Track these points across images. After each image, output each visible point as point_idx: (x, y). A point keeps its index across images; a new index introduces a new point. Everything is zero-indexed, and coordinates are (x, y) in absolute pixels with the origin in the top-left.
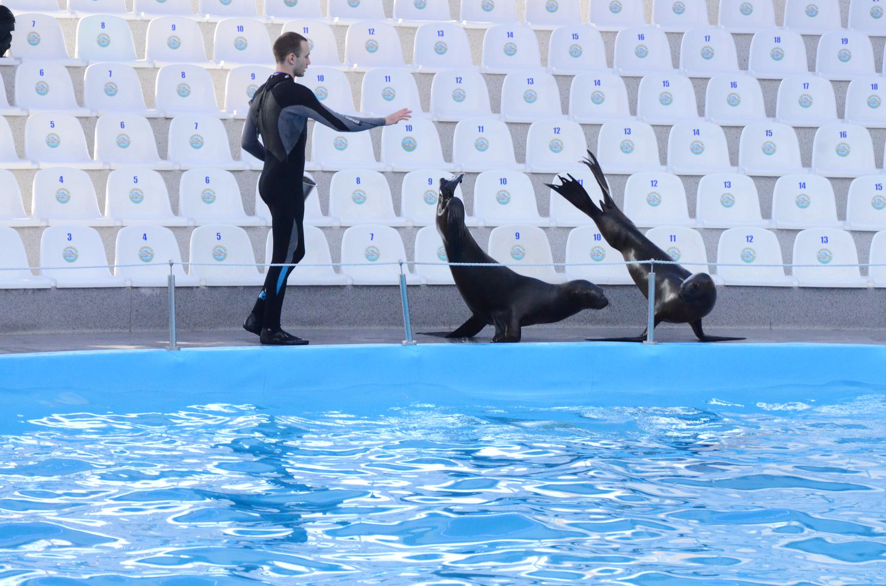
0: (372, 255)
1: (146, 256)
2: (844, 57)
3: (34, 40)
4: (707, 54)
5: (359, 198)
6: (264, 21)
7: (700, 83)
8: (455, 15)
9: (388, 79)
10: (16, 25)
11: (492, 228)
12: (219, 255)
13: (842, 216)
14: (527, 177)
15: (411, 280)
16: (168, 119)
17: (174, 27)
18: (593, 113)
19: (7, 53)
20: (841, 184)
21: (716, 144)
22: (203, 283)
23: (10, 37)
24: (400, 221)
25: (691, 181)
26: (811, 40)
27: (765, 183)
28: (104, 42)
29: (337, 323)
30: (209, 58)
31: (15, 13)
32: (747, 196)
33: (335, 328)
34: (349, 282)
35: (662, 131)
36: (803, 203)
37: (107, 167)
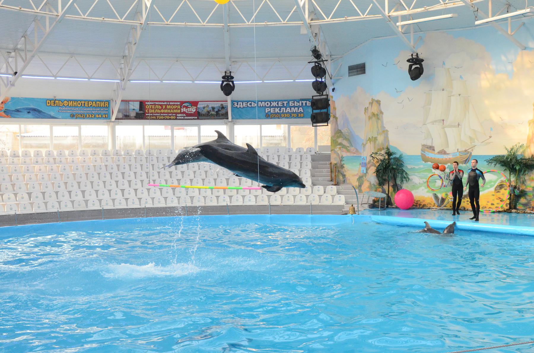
0: (53, 207)
1: (11, 209)
2: (136, 168)
4: (112, 169)
5: (50, 197)
7: (111, 174)
12: (25, 208)
13: (136, 195)
18: (105, 179)
20: (136, 190)
21: (114, 184)
25: (110, 191)
26: (130, 165)
27: (123, 191)
32: (120, 193)
35: (104, 182)
36: (129, 194)
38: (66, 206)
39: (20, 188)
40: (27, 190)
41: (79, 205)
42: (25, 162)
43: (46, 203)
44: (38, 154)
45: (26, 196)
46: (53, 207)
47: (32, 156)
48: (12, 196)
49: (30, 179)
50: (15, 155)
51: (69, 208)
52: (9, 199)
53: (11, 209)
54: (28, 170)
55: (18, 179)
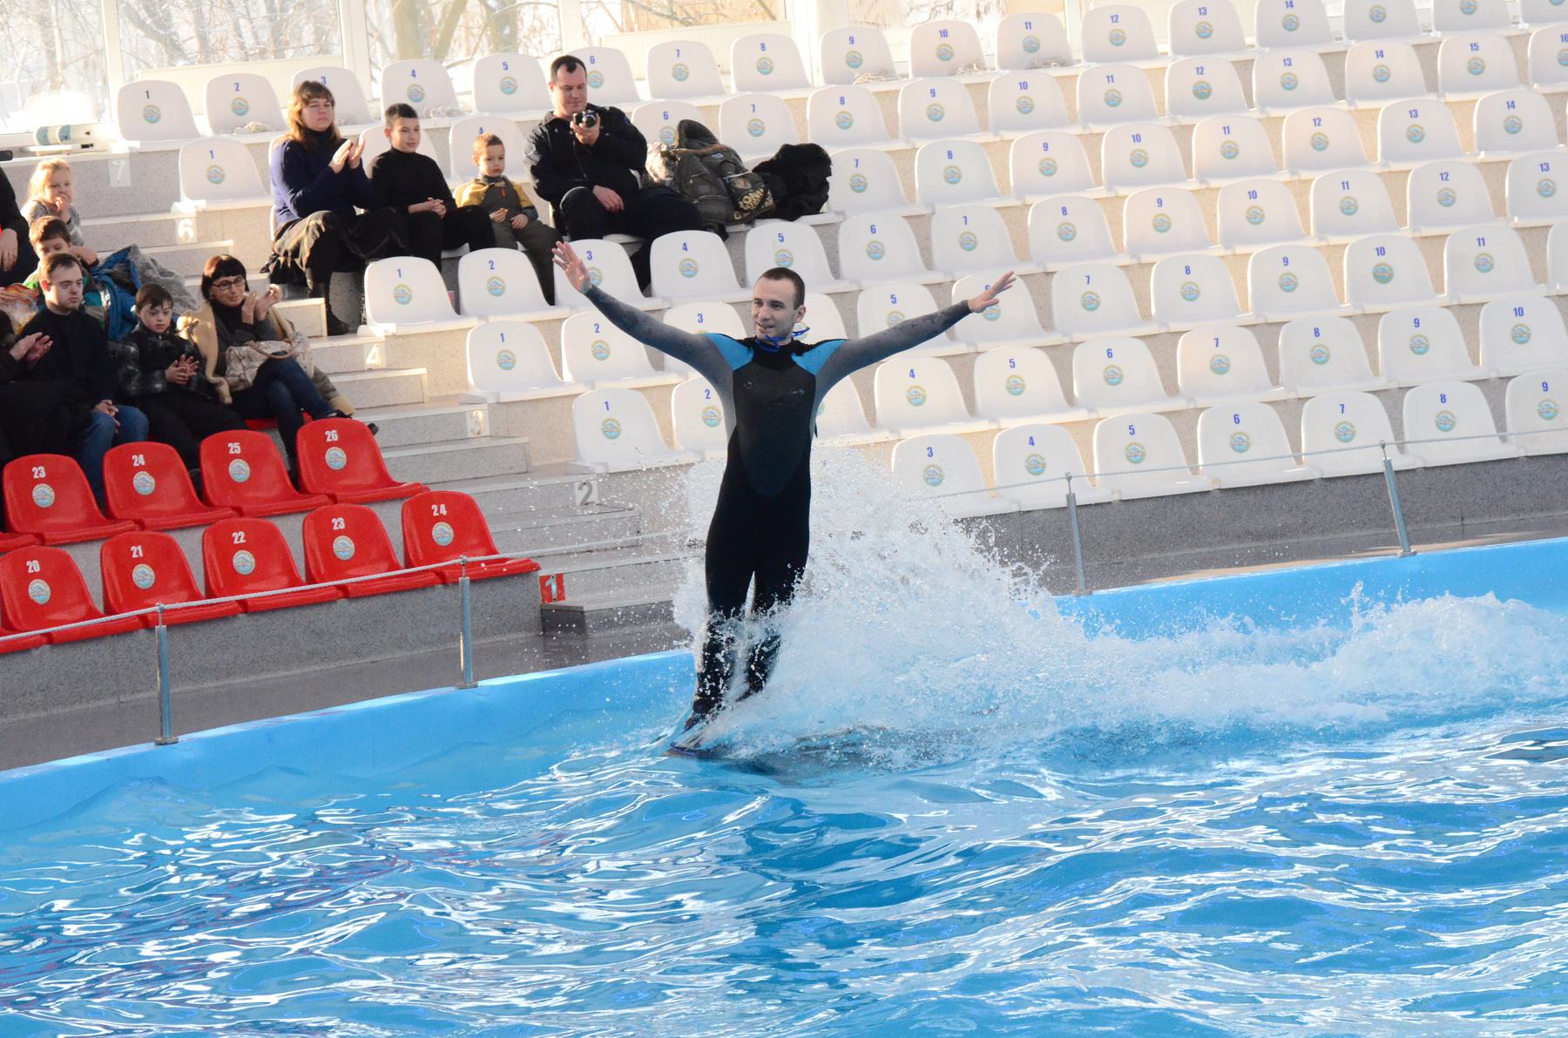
0: (1345, 434)
1: (1036, 467)
3: (859, 185)
5: (1320, 357)
6: (1168, 123)
8: (1432, 86)
9: (1345, 185)
10: (833, 168)
11: (1509, 378)
12: (1136, 455)
14: (1550, 303)
15: (1400, 463)
16: (1049, 274)
17: (1046, 147)
19: (824, 208)
22: (1116, 497)
23: (827, 184)
24: (1380, 384)
28: (953, 177)
29: (1305, 532)
30: (1099, 183)
31: (831, 152)
33: (1305, 539)
34: (1317, 476)
37: (972, 350)
38: (1445, 423)
39: (1091, 303)
40: (1146, 316)
41: (1548, 412)
42: (1113, 100)
43: (1290, 411)
44: (1204, 32)
45: (1139, 365)
46: (1345, 434)
47: (1164, 47)
48: (1039, 373)
49: (1162, 225)
50: (1034, 54)
51: (1472, 440)
52: (1016, 388)
53: (1036, 467)
54: (1139, 160)
55: (1067, 234)
